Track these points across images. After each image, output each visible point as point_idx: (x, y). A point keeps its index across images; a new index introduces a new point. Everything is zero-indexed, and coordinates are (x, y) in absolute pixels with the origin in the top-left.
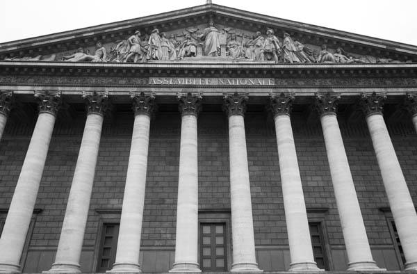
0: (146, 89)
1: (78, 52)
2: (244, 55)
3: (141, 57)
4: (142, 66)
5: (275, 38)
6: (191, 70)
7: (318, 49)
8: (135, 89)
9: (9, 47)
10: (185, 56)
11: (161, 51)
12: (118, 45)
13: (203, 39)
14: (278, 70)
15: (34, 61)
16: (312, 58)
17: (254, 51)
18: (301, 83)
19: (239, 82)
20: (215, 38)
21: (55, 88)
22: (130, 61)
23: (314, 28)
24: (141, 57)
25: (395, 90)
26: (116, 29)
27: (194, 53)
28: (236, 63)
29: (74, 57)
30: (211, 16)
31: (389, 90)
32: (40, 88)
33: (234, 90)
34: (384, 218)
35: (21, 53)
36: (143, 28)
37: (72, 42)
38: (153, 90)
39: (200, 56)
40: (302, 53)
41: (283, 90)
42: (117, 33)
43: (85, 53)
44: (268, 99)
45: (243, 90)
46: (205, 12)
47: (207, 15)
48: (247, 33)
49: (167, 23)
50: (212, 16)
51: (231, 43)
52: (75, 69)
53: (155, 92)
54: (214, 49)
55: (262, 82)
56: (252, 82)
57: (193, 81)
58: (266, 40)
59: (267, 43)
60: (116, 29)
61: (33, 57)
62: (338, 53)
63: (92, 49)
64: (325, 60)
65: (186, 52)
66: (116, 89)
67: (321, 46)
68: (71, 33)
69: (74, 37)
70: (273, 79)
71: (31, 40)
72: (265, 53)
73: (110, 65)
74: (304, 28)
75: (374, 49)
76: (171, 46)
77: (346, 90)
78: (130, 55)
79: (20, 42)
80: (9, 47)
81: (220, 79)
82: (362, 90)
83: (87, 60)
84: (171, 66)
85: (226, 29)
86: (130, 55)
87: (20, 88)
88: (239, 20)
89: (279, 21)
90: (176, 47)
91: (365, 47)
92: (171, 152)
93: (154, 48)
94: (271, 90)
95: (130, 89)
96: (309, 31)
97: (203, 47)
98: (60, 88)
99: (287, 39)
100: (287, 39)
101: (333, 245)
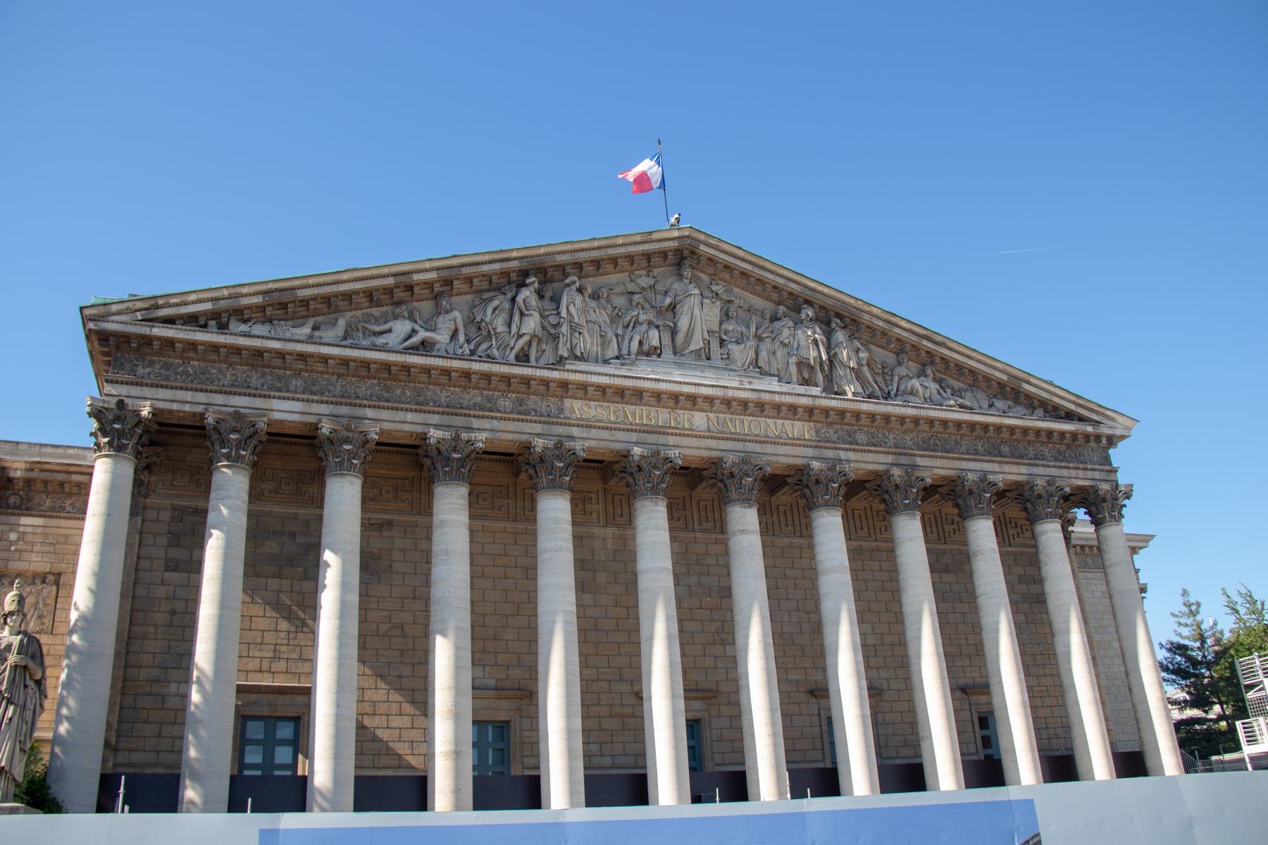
0: (561, 430)
1: (395, 318)
2: (757, 360)
3: (544, 346)
4: (555, 375)
6: (658, 396)
7: (891, 359)
8: (538, 428)
9: (243, 296)
10: (640, 352)
11: (587, 336)
12: (489, 311)
13: (672, 308)
14: (826, 411)
15: (293, 338)
16: (879, 379)
17: (774, 353)
20: (697, 312)
21: (359, 412)
23: (890, 319)
24: (544, 346)
25: (1014, 469)
26: (486, 268)
27: (656, 348)
28: (748, 386)
29: (390, 331)
30: (686, 253)
31: (1007, 468)
32: (324, 409)
33: (739, 446)
34: (967, 707)
35: (269, 311)
37: (389, 291)
38: (575, 432)
39: (667, 353)
40: (865, 369)
41: (831, 454)
42: (488, 277)
43: (411, 318)
44: (802, 471)
45: (757, 448)
46: (675, 244)
47: (678, 251)
48: (759, 303)
49: (597, 263)
50: (684, 256)
51: (730, 328)
52: (406, 368)
54: (697, 343)
56: (772, 426)
57: (662, 416)
60: (486, 268)
61: (298, 320)
62: (926, 376)
64: (904, 393)
65: (641, 343)
66: (495, 423)
67: (898, 354)
68: (386, 271)
69: (391, 281)
70: (812, 424)
71: (296, 283)
72: (799, 364)
73: (485, 367)
74: (870, 313)
75: (987, 379)
76: (603, 317)
77: (939, 463)
78: (522, 342)
79: (271, 286)
80: (243, 296)
81: (712, 415)
82: (964, 465)
84: (617, 381)
85: (714, 288)
86: (522, 342)
87: (276, 404)
88: (744, 274)
89: (826, 290)
90: (615, 318)
91: (973, 372)
92: (582, 561)
93: (574, 328)
94: (810, 452)
95: (527, 428)
96: (881, 324)
97: (674, 332)
98: (370, 413)
99: (840, 336)
100: (840, 336)
101: (887, 758)
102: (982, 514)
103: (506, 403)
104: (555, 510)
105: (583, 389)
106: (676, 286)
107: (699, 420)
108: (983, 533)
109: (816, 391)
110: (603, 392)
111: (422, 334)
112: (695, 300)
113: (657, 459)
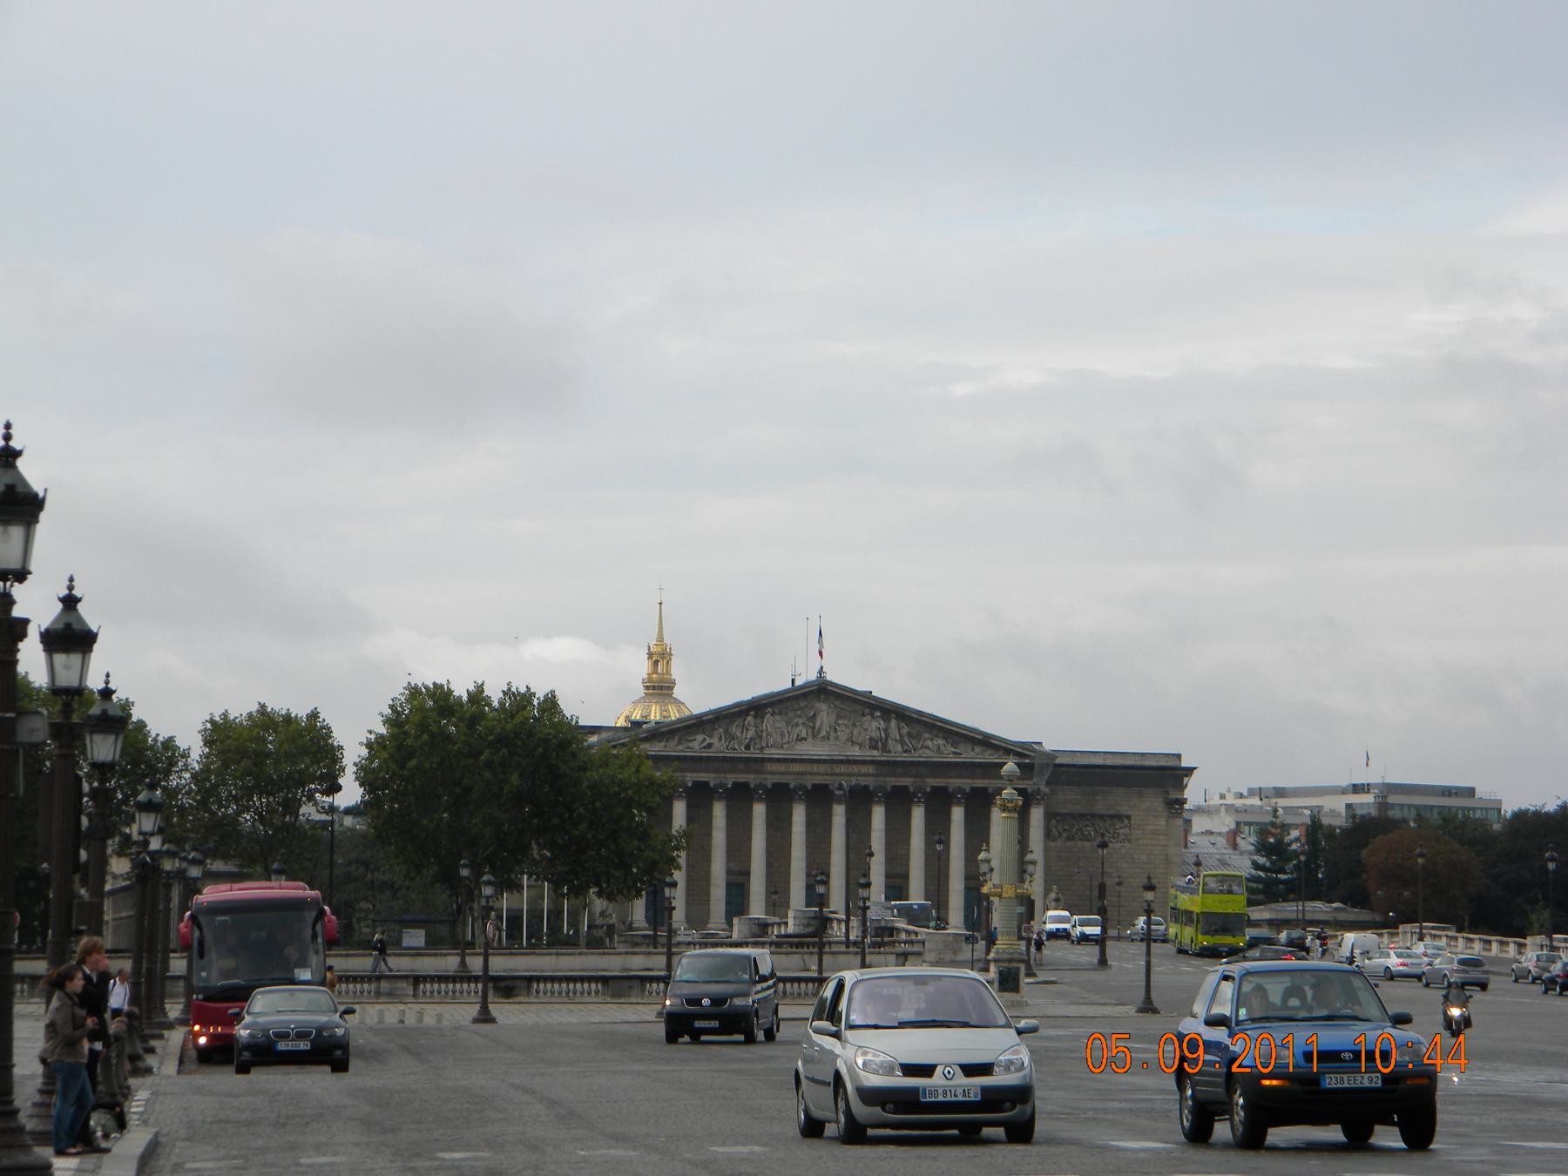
5: (882, 724)
18: (900, 770)
19: (842, 769)
22: (747, 747)
23: (920, 713)
36: (757, 708)
48: (858, 707)
50: (822, 690)
53: (770, 780)
55: (864, 769)
56: (855, 769)
58: (874, 724)
59: (874, 726)
63: (709, 727)
83: (710, 746)
99: (893, 724)
100: (893, 724)
102: (959, 803)
103: (741, 766)
104: (759, 810)
105: (771, 760)
106: (818, 705)
107: (822, 768)
108: (958, 813)
109: (875, 753)
110: (779, 760)
111: (709, 741)
112: (824, 714)
113: (802, 787)
